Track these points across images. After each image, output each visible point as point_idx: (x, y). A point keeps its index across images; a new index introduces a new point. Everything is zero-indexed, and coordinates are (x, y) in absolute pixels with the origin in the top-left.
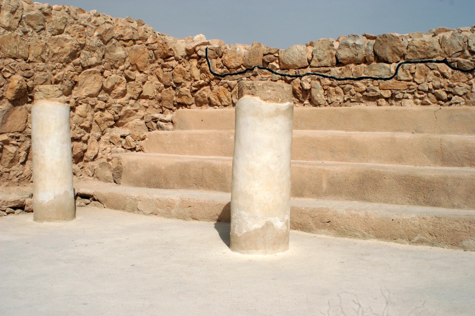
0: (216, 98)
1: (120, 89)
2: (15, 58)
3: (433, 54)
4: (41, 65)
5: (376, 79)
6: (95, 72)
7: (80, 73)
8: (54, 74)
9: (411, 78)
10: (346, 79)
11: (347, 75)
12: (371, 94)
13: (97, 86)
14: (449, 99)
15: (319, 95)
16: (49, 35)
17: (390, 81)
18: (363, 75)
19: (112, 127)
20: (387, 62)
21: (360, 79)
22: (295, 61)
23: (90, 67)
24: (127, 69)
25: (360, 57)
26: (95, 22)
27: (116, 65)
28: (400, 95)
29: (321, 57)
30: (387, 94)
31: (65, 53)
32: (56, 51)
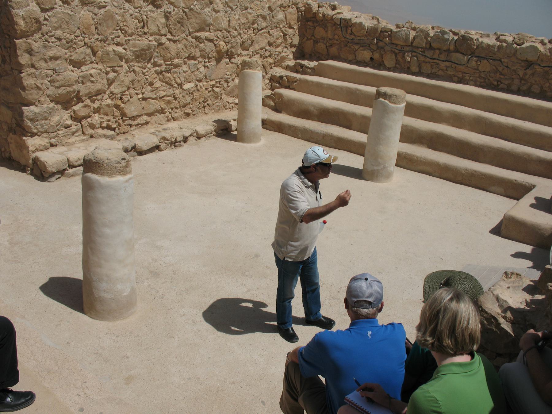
2: (220, 31)
4: (235, 33)
6: (264, 33)
14: (498, 85)
16: (239, 11)
23: (262, 29)
32: (243, 22)
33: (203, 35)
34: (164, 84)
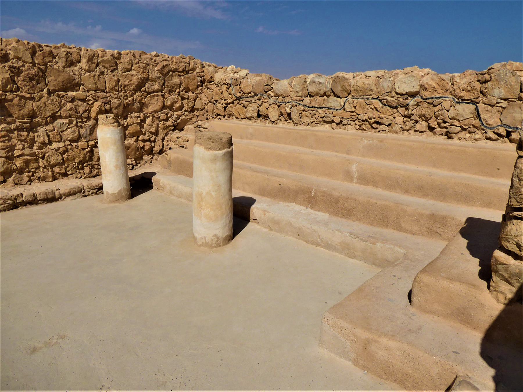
1: (177, 105)
3: (371, 93)
5: (331, 109)
7: (146, 97)
8: (126, 99)
9: (353, 109)
10: (312, 107)
11: (313, 104)
12: (327, 119)
13: (160, 104)
16: (120, 72)
17: (340, 111)
18: (323, 106)
19: (173, 130)
21: (321, 108)
23: (153, 92)
24: (182, 91)
25: (322, 92)
26: (155, 61)
27: (174, 89)
28: (345, 122)
29: (298, 90)
30: (337, 120)
31: (133, 84)
32: (126, 83)
33: (71, 94)
34: (19, 142)
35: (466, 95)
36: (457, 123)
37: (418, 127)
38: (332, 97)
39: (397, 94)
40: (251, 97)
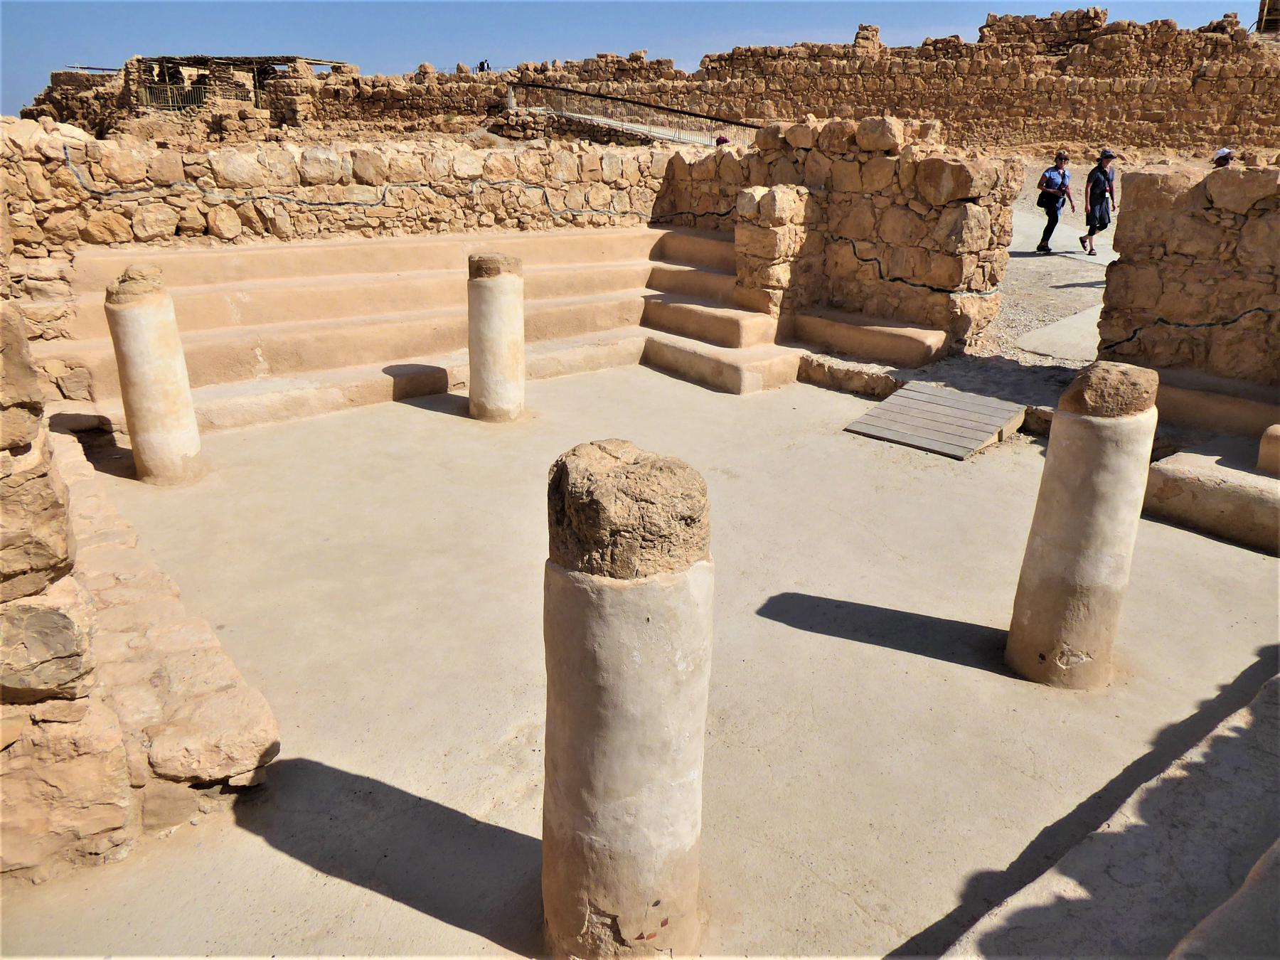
0: (103, 230)
12: (356, 222)
15: (284, 223)
20: (371, 185)
21: (340, 204)
22: (247, 179)
25: (337, 177)
29: (282, 174)
35: (534, 179)
36: (527, 211)
37: (484, 220)
38: (353, 185)
39: (456, 177)
40: (140, 190)
